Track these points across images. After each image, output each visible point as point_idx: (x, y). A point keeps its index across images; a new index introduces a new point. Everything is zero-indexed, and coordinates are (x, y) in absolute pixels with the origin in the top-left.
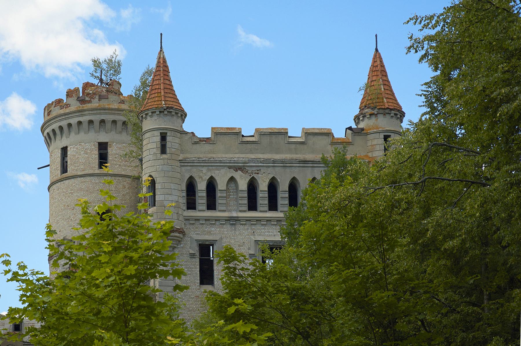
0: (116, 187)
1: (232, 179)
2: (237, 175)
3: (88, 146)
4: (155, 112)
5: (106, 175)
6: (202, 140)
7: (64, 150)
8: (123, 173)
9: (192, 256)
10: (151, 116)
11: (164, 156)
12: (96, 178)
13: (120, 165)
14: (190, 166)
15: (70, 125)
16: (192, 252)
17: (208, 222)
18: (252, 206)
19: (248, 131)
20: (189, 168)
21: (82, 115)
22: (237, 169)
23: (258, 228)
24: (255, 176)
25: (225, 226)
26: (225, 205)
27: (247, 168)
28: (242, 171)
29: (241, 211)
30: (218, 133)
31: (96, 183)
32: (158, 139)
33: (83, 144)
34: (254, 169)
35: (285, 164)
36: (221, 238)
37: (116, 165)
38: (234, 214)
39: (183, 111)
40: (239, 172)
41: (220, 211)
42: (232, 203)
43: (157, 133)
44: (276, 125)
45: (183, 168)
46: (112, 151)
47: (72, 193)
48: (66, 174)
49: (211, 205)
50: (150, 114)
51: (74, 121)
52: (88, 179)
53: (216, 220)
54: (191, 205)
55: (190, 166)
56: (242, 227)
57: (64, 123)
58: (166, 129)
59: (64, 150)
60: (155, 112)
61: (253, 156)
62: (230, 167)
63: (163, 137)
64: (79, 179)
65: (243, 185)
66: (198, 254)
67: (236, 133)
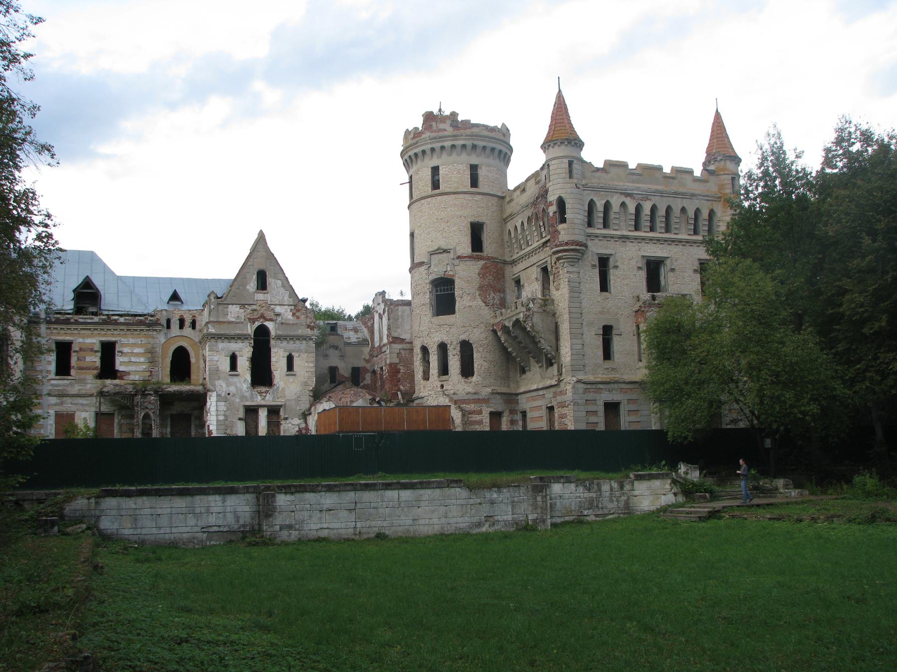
0: (486, 205)
1: (623, 205)
2: (628, 201)
3: (460, 167)
4: (556, 143)
5: (479, 194)
6: (598, 170)
7: (435, 170)
8: (492, 193)
9: (594, 266)
10: (559, 146)
11: (571, 180)
12: (469, 195)
13: (488, 186)
14: (591, 190)
15: (443, 148)
16: (593, 263)
17: (605, 239)
18: (637, 228)
19: (632, 166)
20: (590, 192)
21: (456, 140)
22: (627, 195)
23: (643, 245)
24: (641, 202)
25: (618, 243)
27: (634, 195)
28: (631, 197)
29: (629, 231)
30: (611, 165)
31: (469, 200)
32: (567, 165)
33: (455, 165)
34: (640, 196)
35: (662, 194)
36: (616, 253)
37: (485, 185)
38: (626, 233)
39: (581, 141)
40: (629, 198)
41: (598, 229)
42: (622, 224)
43: (566, 161)
44: (655, 162)
45: (586, 192)
46: (482, 173)
47: (446, 208)
48: (438, 190)
49: (606, 225)
50: (552, 145)
51: (447, 144)
52: (461, 196)
53: (612, 237)
54: (590, 224)
55: (591, 190)
56: (631, 244)
57: (437, 146)
58: (573, 157)
59: (435, 170)
60: (556, 143)
61: (637, 185)
62: (621, 194)
63: (570, 164)
64: (452, 195)
65: (632, 208)
66: (598, 265)
67: (623, 165)
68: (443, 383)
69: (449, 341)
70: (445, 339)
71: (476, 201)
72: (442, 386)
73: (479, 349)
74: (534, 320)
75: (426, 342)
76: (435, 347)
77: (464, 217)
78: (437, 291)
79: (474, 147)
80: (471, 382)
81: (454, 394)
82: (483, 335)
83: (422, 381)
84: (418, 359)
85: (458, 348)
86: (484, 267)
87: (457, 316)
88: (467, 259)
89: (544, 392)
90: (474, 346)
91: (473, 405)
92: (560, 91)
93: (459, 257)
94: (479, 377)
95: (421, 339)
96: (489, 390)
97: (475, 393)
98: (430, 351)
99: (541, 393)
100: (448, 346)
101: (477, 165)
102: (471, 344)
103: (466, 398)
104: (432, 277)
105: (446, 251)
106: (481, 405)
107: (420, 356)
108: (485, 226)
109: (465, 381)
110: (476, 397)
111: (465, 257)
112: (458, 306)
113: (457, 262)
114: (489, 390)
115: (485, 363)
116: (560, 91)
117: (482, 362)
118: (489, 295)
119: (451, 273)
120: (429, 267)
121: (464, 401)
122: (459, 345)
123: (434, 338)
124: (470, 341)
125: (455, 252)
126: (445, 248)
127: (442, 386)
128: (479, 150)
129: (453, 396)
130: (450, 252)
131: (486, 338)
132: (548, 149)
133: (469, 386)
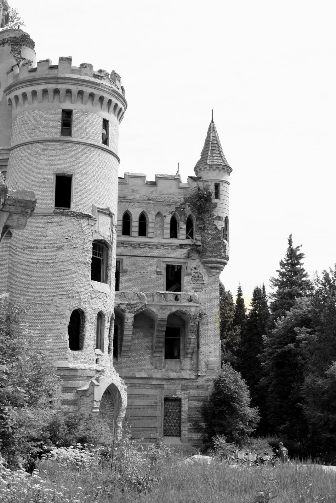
26: (153, 233)
68: (99, 357)
76: (95, 316)
89: (163, 382)
92: (212, 121)
98: (88, 318)
104: (97, 237)
105: (110, 215)
116: (212, 121)
127: (97, 361)
132: (214, 170)
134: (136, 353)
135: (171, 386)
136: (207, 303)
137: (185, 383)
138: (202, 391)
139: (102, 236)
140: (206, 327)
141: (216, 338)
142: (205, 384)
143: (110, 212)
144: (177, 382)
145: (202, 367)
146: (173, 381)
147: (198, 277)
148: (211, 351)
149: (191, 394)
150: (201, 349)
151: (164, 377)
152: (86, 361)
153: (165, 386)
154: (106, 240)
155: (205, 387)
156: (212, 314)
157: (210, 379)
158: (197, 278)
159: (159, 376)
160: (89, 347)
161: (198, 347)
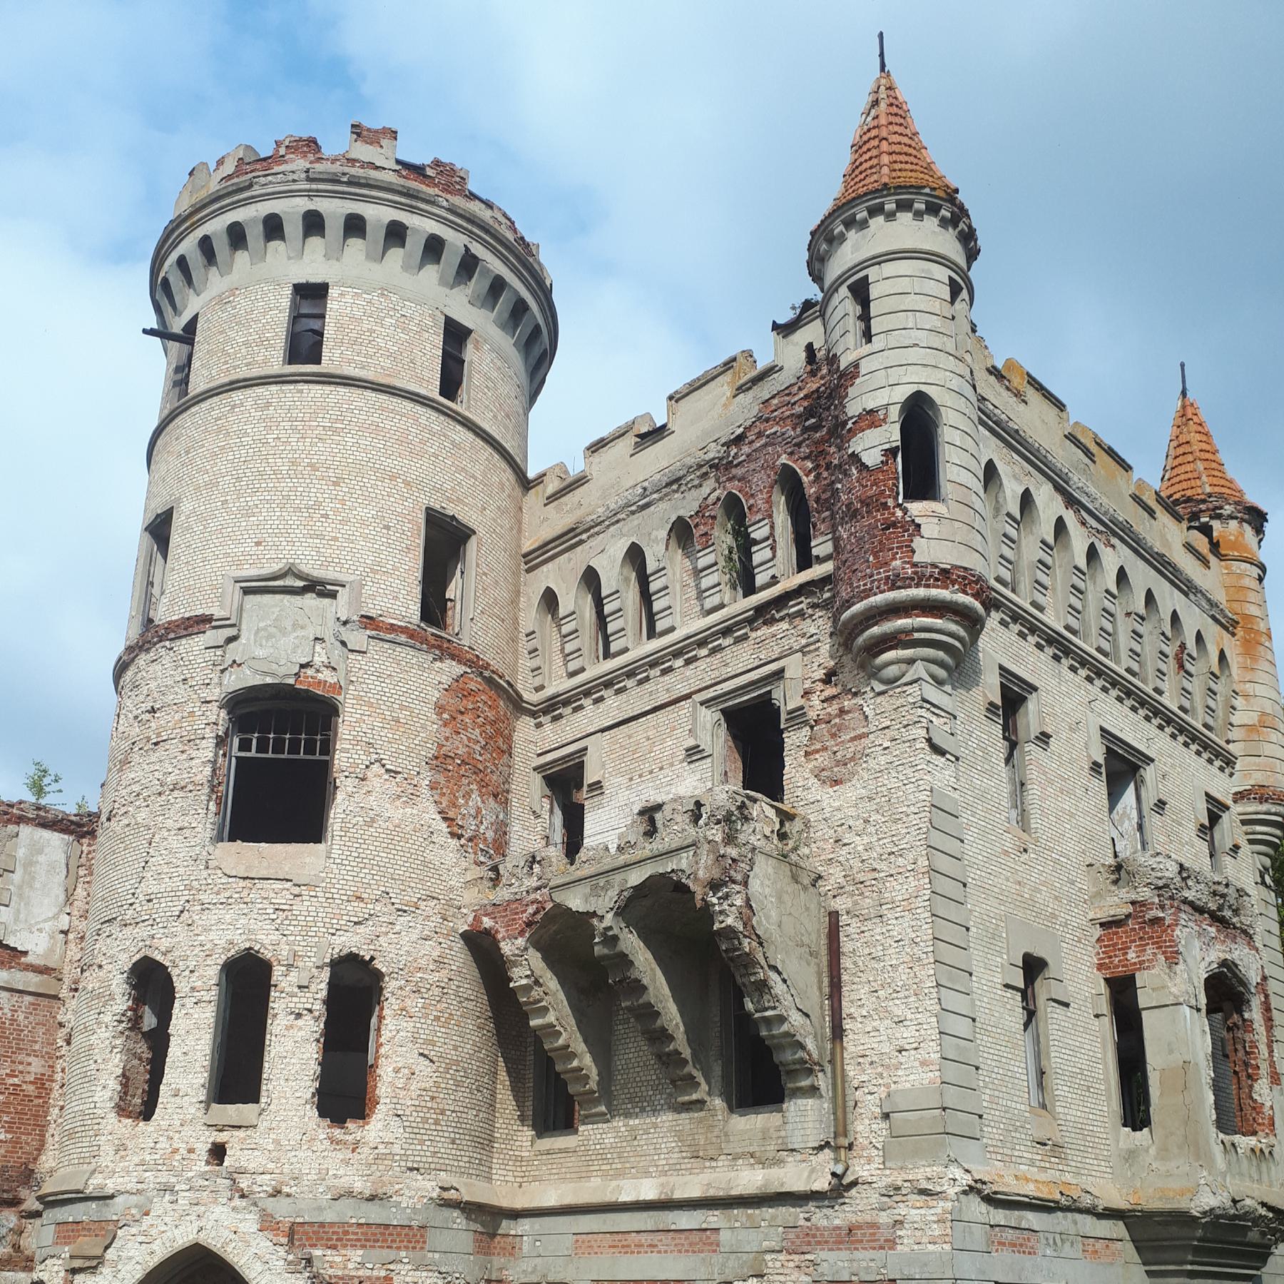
12: (434, 415)
69: (284, 952)
70: (266, 941)
71: (453, 442)
72: (218, 1152)
73: (408, 1002)
74: (755, 885)
75: (165, 944)
76: (211, 973)
77: (407, 483)
78: (245, 746)
79: (468, 265)
80: (355, 1147)
81: (277, 1193)
82: (431, 950)
83: (112, 1117)
84: (107, 1018)
85: (321, 988)
86: (457, 688)
87: (336, 852)
88: (403, 638)
89: (713, 1218)
90: (390, 986)
91: (356, 1255)
93: (369, 621)
94: (394, 1122)
95: (142, 932)
96: (429, 1185)
97: (372, 1198)
98: (181, 986)
99: (685, 1220)
100: (277, 972)
101: (469, 332)
102: (379, 976)
103: (329, 1217)
105: (318, 587)
106: (392, 1254)
107: (122, 1004)
108: (472, 544)
109: (332, 1140)
110: (374, 1214)
111: (393, 628)
112: (340, 810)
113: (357, 638)
114: (428, 1186)
115: (423, 1066)
117: (413, 1059)
118: (467, 795)
119: (327, 675)
120: (231, 640)
121: (333, 1235)
122: (326, 974)
123: (207, 930)
124: (379, 965)
125: (357, 599)
126: (318, 573)
127: (218, 1152)
128: (478, 284)
129: (270, 1204)
130: (333, 595)
131: (439, 962)
133: (347, 1162)
134: (631, 1100)
135: (743, 1234)
136: (874, 817)
137: (797, 1217)
138: (871, 1254)
139: (266, 673)
140: (878, 930)
141: (922, 974)
142: (884, 1218)
143: (299, 576)
144: (768, 1212)
145: (866, 1128)
146: (750, 1211)
147: (842, 712)
148: (902, 1043)
149: (824, 1267)
150: (851, 1044)
151: (712, 1193)
152: (157, 1157)
153: (724, 1236)
154: (291, 681)
155: (885, 1234)
156: (900, 861)
157: (898, 1189)
158: (837, 720)
159: (695, 1192)
160: (178, 1100)
161: (838, 1032)
